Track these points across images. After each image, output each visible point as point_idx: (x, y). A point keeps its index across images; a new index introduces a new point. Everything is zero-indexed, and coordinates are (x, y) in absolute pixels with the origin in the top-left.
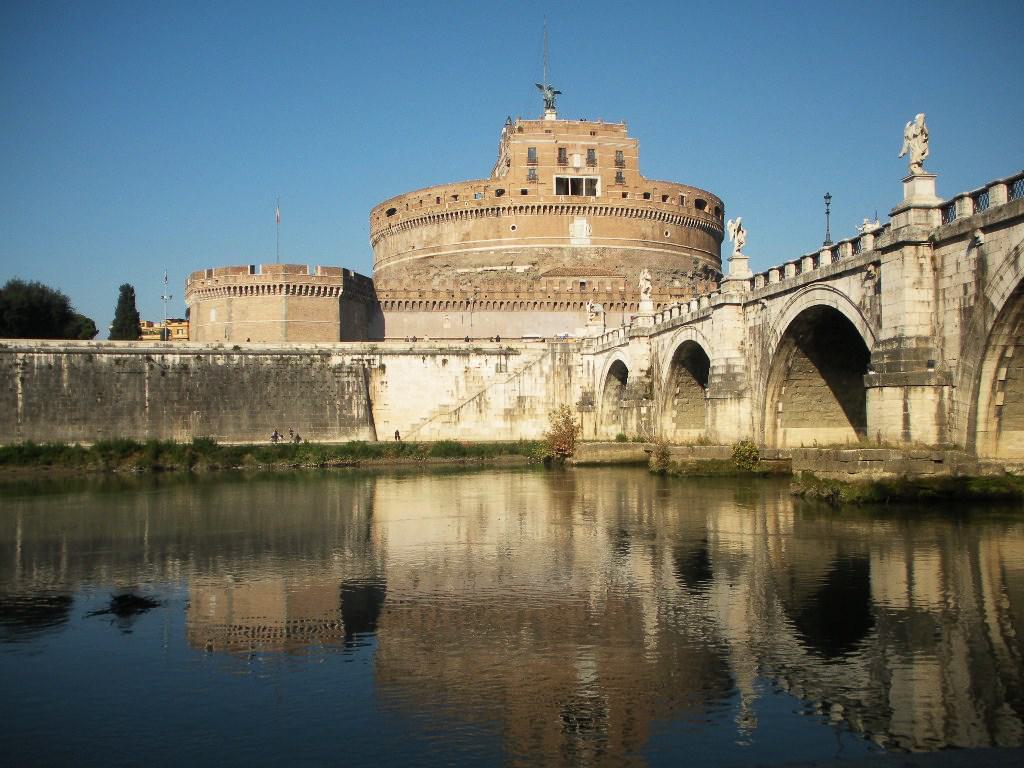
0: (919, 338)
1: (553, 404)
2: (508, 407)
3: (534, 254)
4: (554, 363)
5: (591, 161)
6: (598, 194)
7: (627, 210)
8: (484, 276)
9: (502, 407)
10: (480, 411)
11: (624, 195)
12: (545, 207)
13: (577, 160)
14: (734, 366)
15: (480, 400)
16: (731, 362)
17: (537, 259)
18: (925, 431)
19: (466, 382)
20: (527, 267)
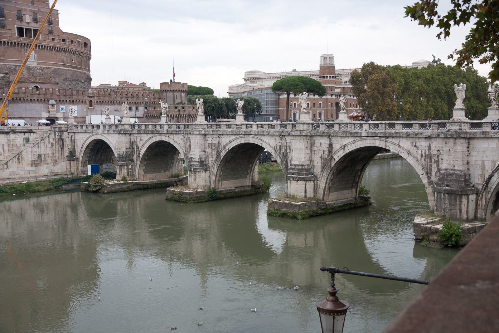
0: (308, 165)
1: (55, 157)
2: (33, 160)
3: (6, 68)
4: (55, 137)
5: (35, 20)
7: (55, 47)
9: (30, 160)
10: (19, 162)
11: (53, 39)
12: (12, 43)
13: (28, 18)
14: (203, 158)
15: (19, 157)
16: (201, 156)
17: (7, 71)
18: (310, 194)
19: (8, 147)
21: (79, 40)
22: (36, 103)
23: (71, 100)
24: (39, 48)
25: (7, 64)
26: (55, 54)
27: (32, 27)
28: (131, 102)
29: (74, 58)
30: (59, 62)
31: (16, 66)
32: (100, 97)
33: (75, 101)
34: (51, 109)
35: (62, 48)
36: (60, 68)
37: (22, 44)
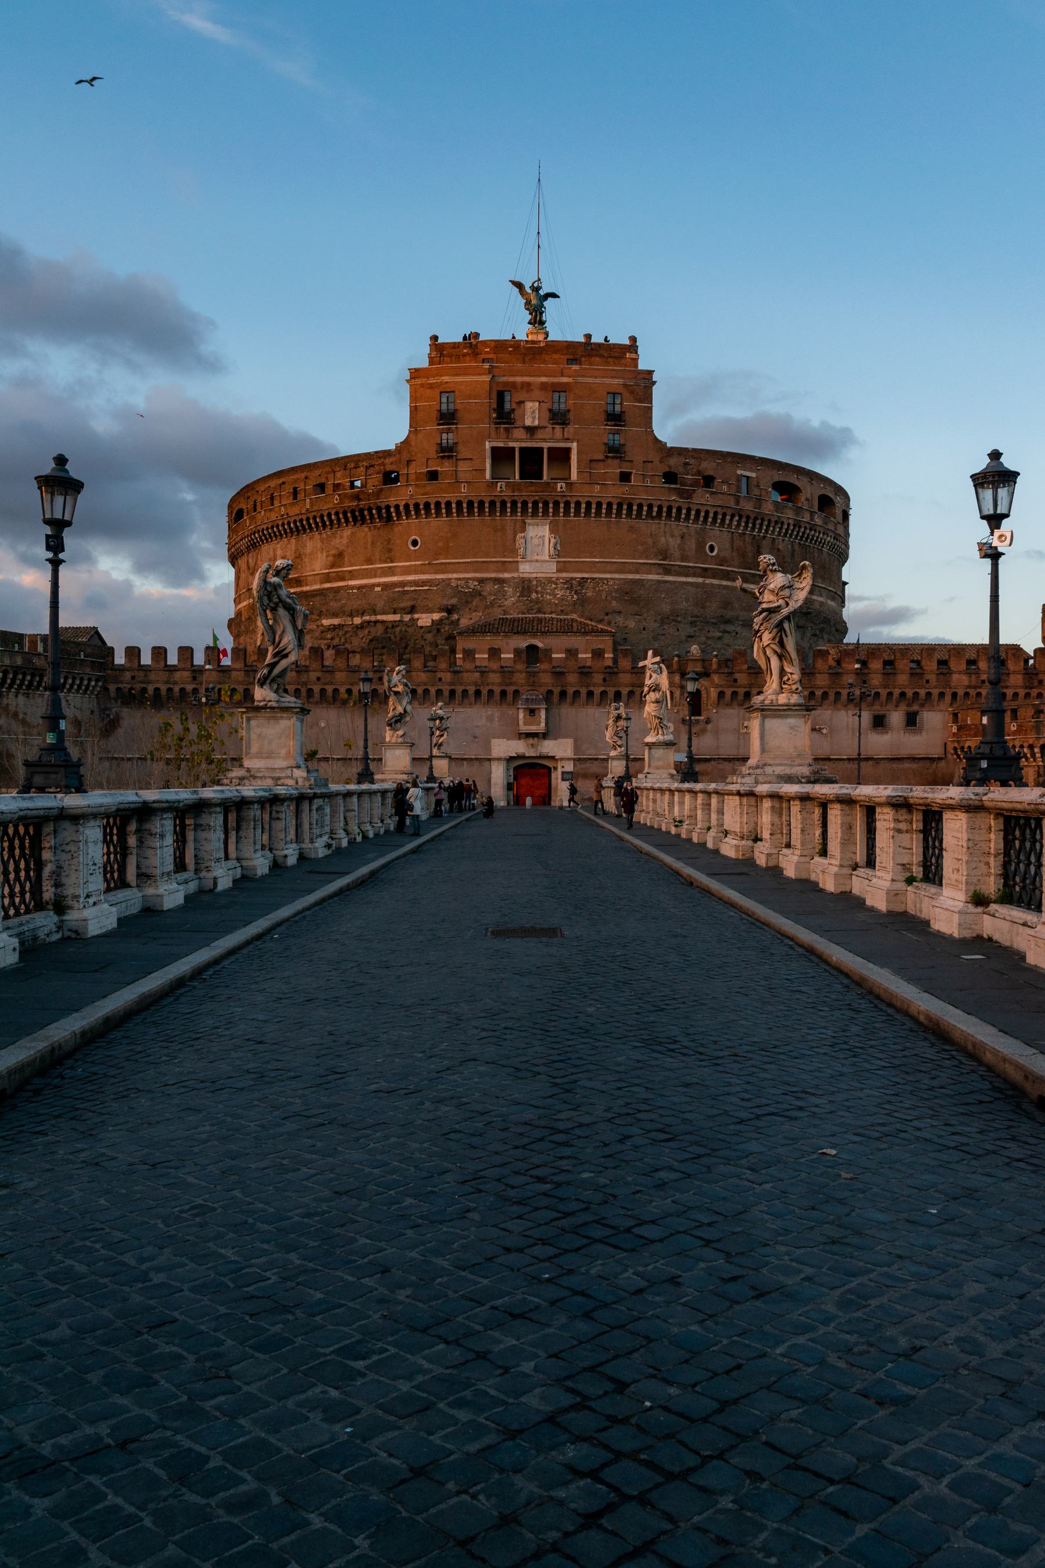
3: (449, 591)
5: (559, 418)
6: (574, 476)
7: (630, 506)
8: (366, 631)
11: (625, 477)
12: (470, 504)
13: (532, 413)
17: (454, 601)
20: (436, 616)
21: (748, 474)
22: (470, 704)
23: (611, 691)
24: (567, 512)
25: (455, 576)
26: (632, 529)
27: (544, 440)
28: (884, 693)
29: (719, 541)
30: (647, 558)
31: (481, 581)
32: (737, 676)
33: (625, 691)
34: (525, 724)
35: (660, 507)
36: (651, 577)
37: (503, 503)
